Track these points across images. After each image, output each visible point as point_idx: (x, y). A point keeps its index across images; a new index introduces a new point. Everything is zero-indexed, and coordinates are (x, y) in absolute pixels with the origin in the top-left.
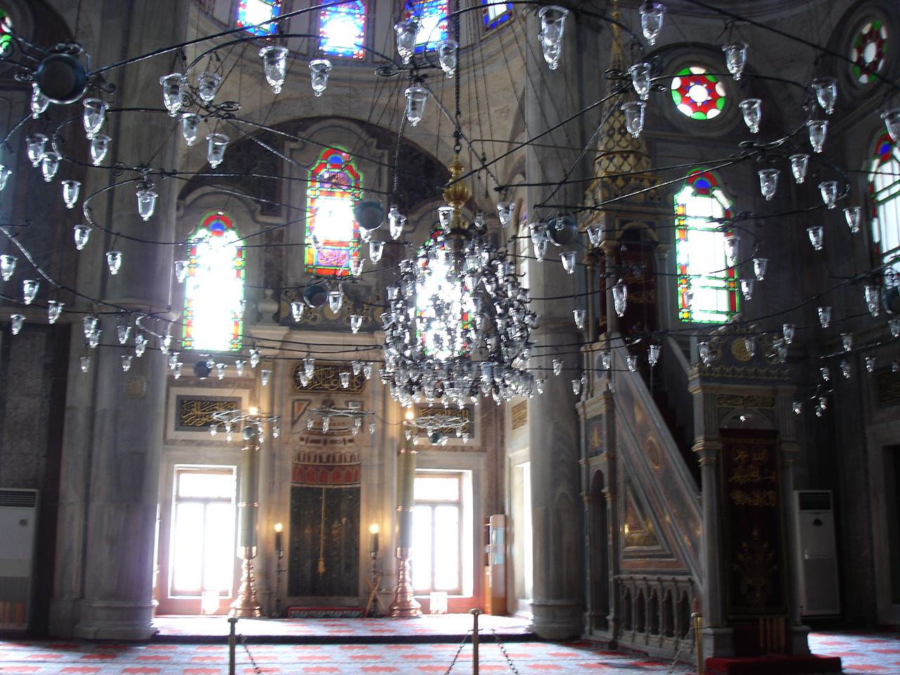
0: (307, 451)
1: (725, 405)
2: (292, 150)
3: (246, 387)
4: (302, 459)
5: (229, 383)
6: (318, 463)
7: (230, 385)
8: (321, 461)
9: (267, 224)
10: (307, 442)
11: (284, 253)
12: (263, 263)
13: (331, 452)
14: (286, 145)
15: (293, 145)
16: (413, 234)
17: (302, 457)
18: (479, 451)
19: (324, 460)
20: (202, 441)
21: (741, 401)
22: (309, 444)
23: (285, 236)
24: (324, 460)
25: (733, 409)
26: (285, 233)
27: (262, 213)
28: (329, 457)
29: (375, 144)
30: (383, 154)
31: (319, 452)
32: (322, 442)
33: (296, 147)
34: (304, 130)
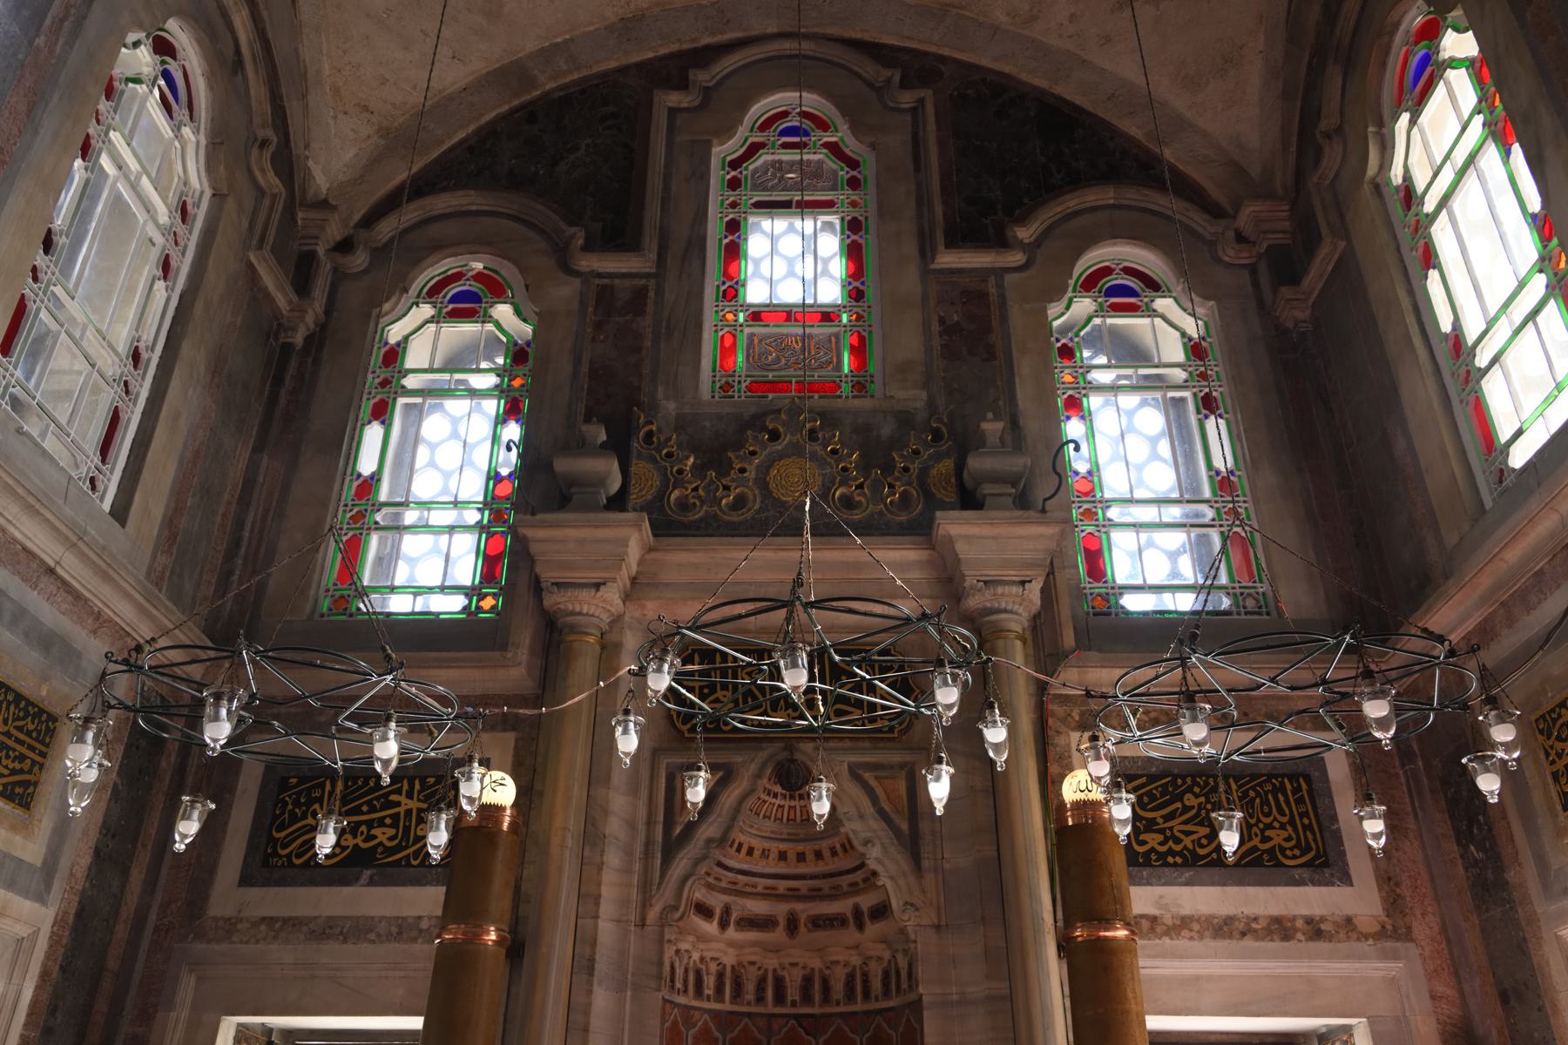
0: (729, 960)
2: (673, 112)
4: (709, 991)
6: (770, 1007)
8: (780, 998)
9: (600, 275)
10: (723, 925)
12: (585, 369)
13: (816, 963)
14: (656, 99)
15: (674, 99)
16: (1024, 275)
17: (710, 982)
18: (1381, 934)
19: (792, 993)
20: (331, 922)
22: (731, 932)
23: (650, 302)
24: (792, 993)
26: (652, 294)
27: (588, 247)
28: (807, 981)
29: (897, 78)
30: (921, 101)
31: (771, 963)
32: (782, 922)
33: (685, 105)
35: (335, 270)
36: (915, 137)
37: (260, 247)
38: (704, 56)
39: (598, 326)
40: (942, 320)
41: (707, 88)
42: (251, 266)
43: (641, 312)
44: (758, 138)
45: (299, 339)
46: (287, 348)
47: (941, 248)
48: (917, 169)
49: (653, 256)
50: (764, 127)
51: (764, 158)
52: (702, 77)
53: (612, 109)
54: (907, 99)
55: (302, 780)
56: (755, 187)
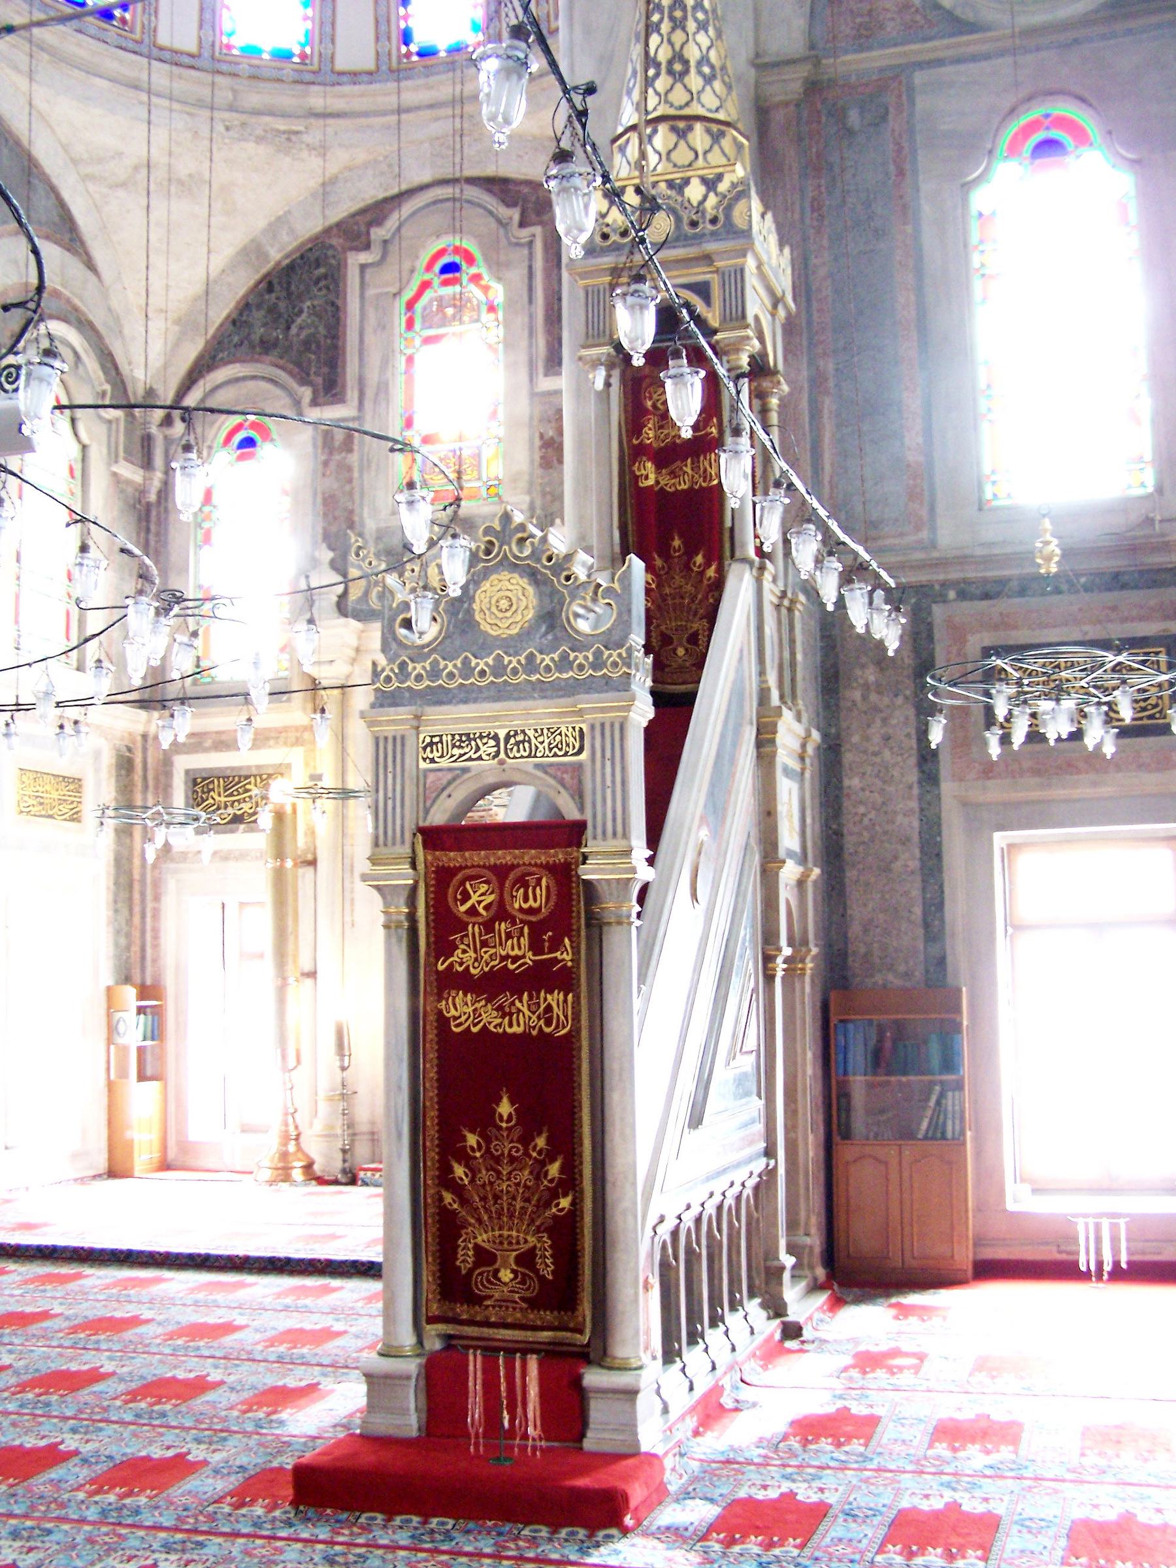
1: (444, 763)
2: (363, 267)
3: (298, 742)
5: (268, 739)
7: (272, 742)
11: (356, 475)
12: (319, 500)
15: (364, 257)
20: (230, 852)
21: (488, 748)
25: (465, 770)
27: (314, 403)
29: (516, 217)
34: (379, 221)
35: (166, 437)
36: (530, 267)
37: (116, 462)
38: (377, 211)
39: (326, 464)
40: (542, 436)
41: (385, 242)
42: (115, 474)
43: (350, 451)
44: (427, 277)
45: (152, 497)
46: (148, 504)
47: (541, 376)
48: (530, 301)
49: (356, 402)
50: (429, 268)
51: (428, 294)
52: (378, 234)
53: (322, 270)
54: (525, 233)
55: (204, 779)
56: (427, 324)
